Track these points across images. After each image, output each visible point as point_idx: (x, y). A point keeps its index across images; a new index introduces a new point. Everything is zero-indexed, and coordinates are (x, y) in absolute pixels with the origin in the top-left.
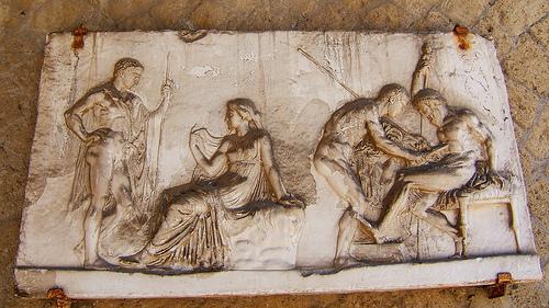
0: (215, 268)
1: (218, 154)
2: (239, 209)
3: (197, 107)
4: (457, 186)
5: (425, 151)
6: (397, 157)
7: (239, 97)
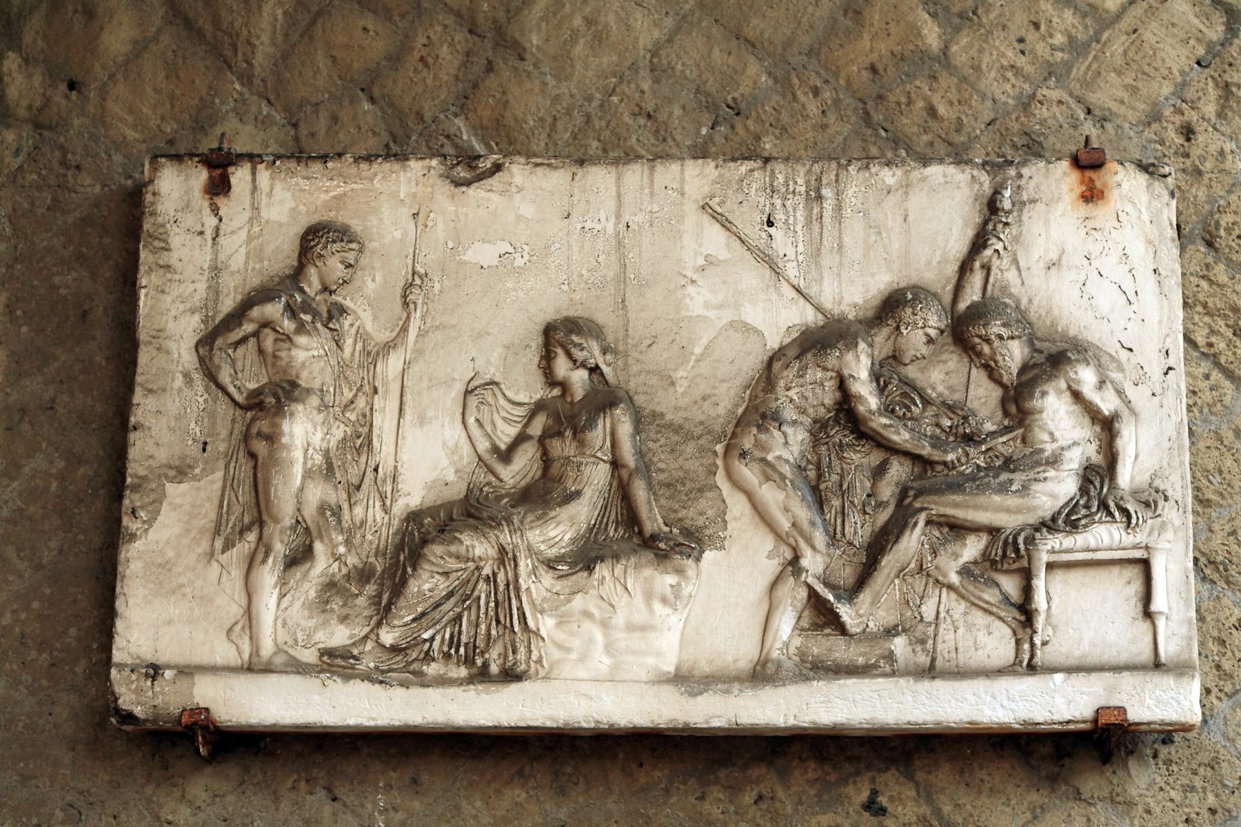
0: (510, 675)
1: (521, 439)
2: (560, 559)
3: (478, 336)
4: (1032, 519)
5: (969, 439)
6: (907, 454)
7: (571, 313)
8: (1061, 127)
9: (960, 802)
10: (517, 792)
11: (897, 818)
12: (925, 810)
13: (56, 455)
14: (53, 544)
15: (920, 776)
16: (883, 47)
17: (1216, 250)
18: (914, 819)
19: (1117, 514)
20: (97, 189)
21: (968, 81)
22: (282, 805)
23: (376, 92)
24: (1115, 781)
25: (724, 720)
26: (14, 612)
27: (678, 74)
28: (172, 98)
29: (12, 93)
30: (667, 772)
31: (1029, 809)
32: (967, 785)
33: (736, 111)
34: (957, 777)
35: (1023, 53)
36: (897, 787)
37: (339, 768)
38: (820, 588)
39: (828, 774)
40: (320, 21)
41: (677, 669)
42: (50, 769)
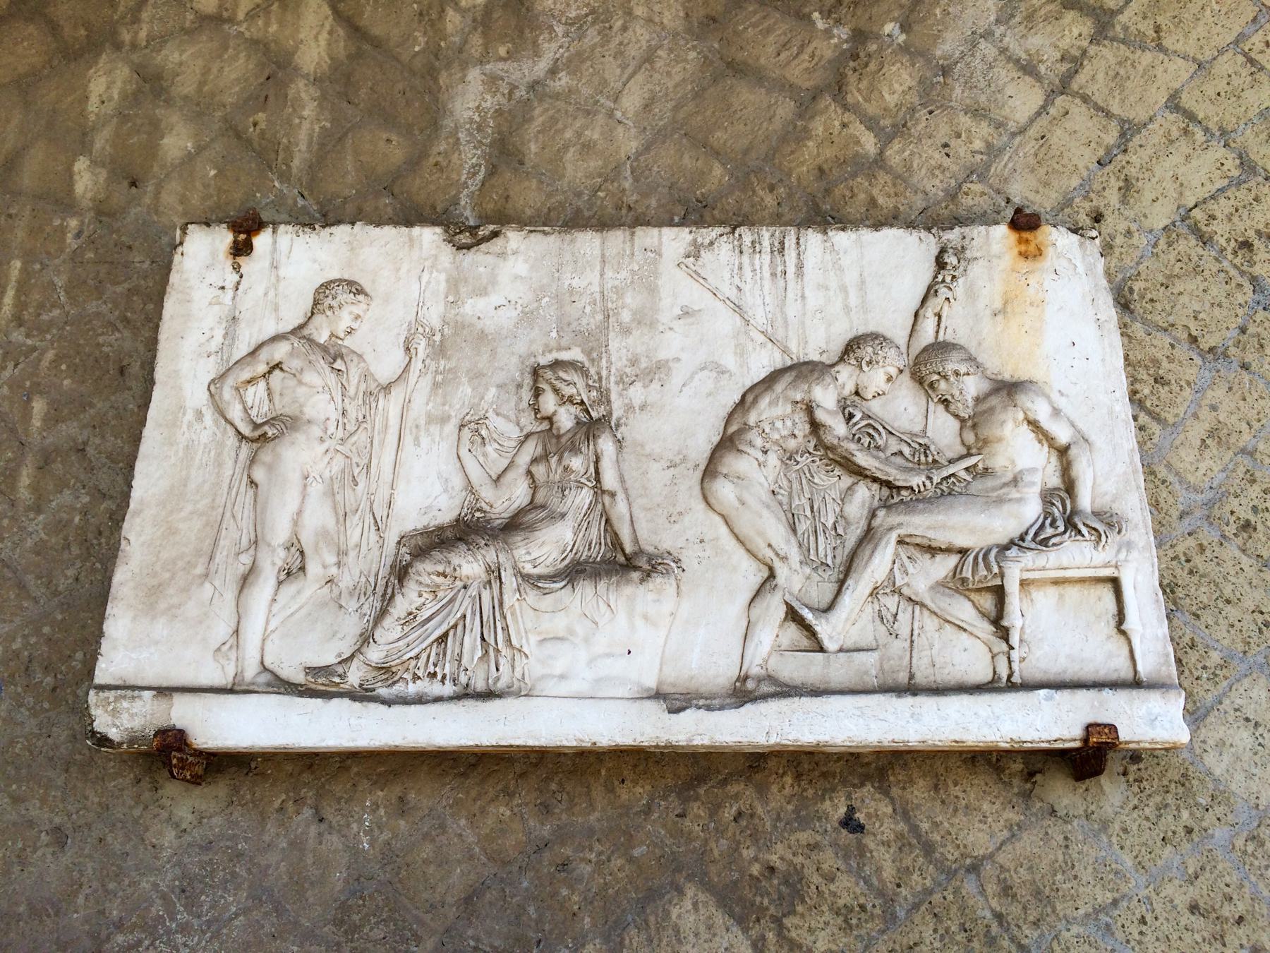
8: (986, 212)
9: (938, 820)
10: (502, 809)
11: (874, 835)
12: (902, 827)
13: (83, 491)
14: (71, 572)
15: (895, 791)
16: (829, 152)
17: (1132, 312)
18: (892, 837)
19: (1086, 533)
20: (146, 265)
21: (901, 178)
22: (269, 826)
23: (396, 191)
24: (1088, 799)
25: (707, 737)
26: (24, 636)
27: (654, 174)
28: (219, 190)
29: (79, 188)
30: (648, 788)
31: (1006, 827)
32: (943, 802)
33: (704, 203)
34: (932, 793)
35: (948, 155)
36: (873, 803)
37: (327, 787)
38: (796, 605)
39: (805, 790)
40: (350, 135)
41: (660, 683)
42: (42, 791)
